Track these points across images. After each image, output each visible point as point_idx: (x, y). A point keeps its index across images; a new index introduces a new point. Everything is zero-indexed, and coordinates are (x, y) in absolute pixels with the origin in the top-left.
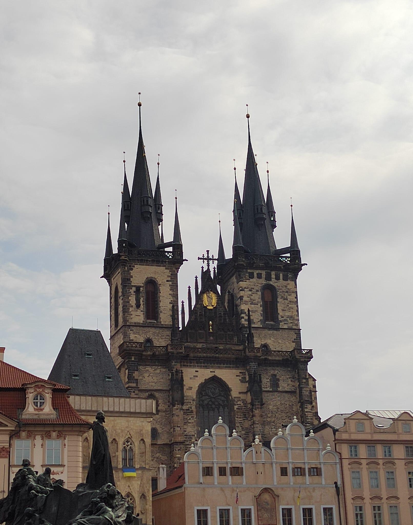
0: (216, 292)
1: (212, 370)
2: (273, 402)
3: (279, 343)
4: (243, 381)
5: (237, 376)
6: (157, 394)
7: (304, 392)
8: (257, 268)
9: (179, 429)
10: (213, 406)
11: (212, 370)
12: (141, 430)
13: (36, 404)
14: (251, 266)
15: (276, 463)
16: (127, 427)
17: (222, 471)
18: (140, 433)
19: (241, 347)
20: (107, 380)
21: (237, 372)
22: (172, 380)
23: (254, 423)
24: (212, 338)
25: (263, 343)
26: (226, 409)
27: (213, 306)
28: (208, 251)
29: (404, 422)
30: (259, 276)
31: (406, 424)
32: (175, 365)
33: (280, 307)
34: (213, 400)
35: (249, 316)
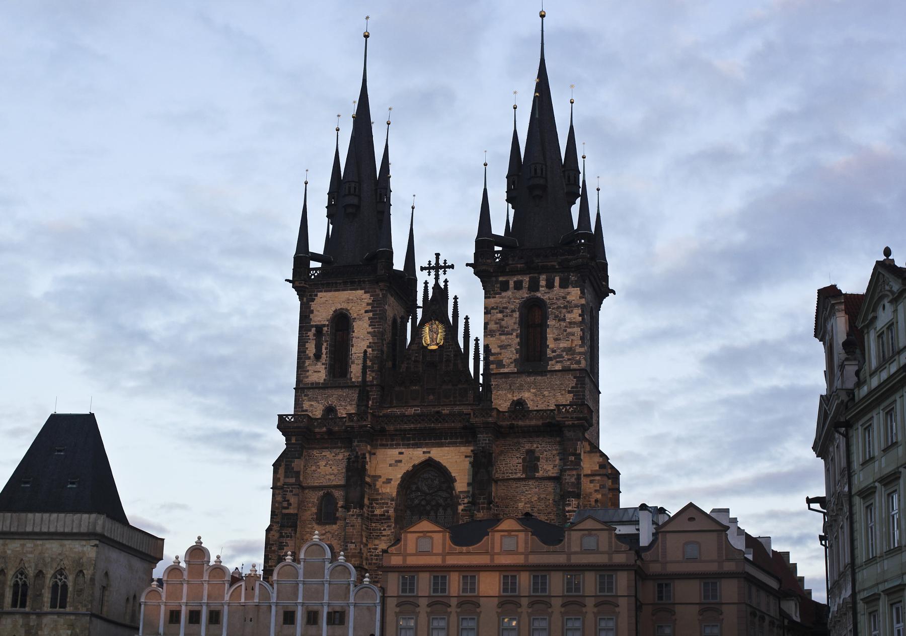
1: (425, 450)
3: (544, 396)
5: (466, 457)
6: (338, 494)
7: (568, 477)
8: (514, 272)
9: (353, 546)
10: (428, 508)
11: (425, 450)
12: (81, 558)
15: (277, 604)
16: (60, 554)
17: (194, 617)
20: (69, 486)
21: (467, 450)
24: (431, 397)
25: (515, 399)
26: (449, 511)
27: (437, 344)
28: (438, 255)
29: (506, 533)
30: (518, 286)
31: (510, 536)
32: (357, 446)
33: (550, 336)
34: (428, 498)
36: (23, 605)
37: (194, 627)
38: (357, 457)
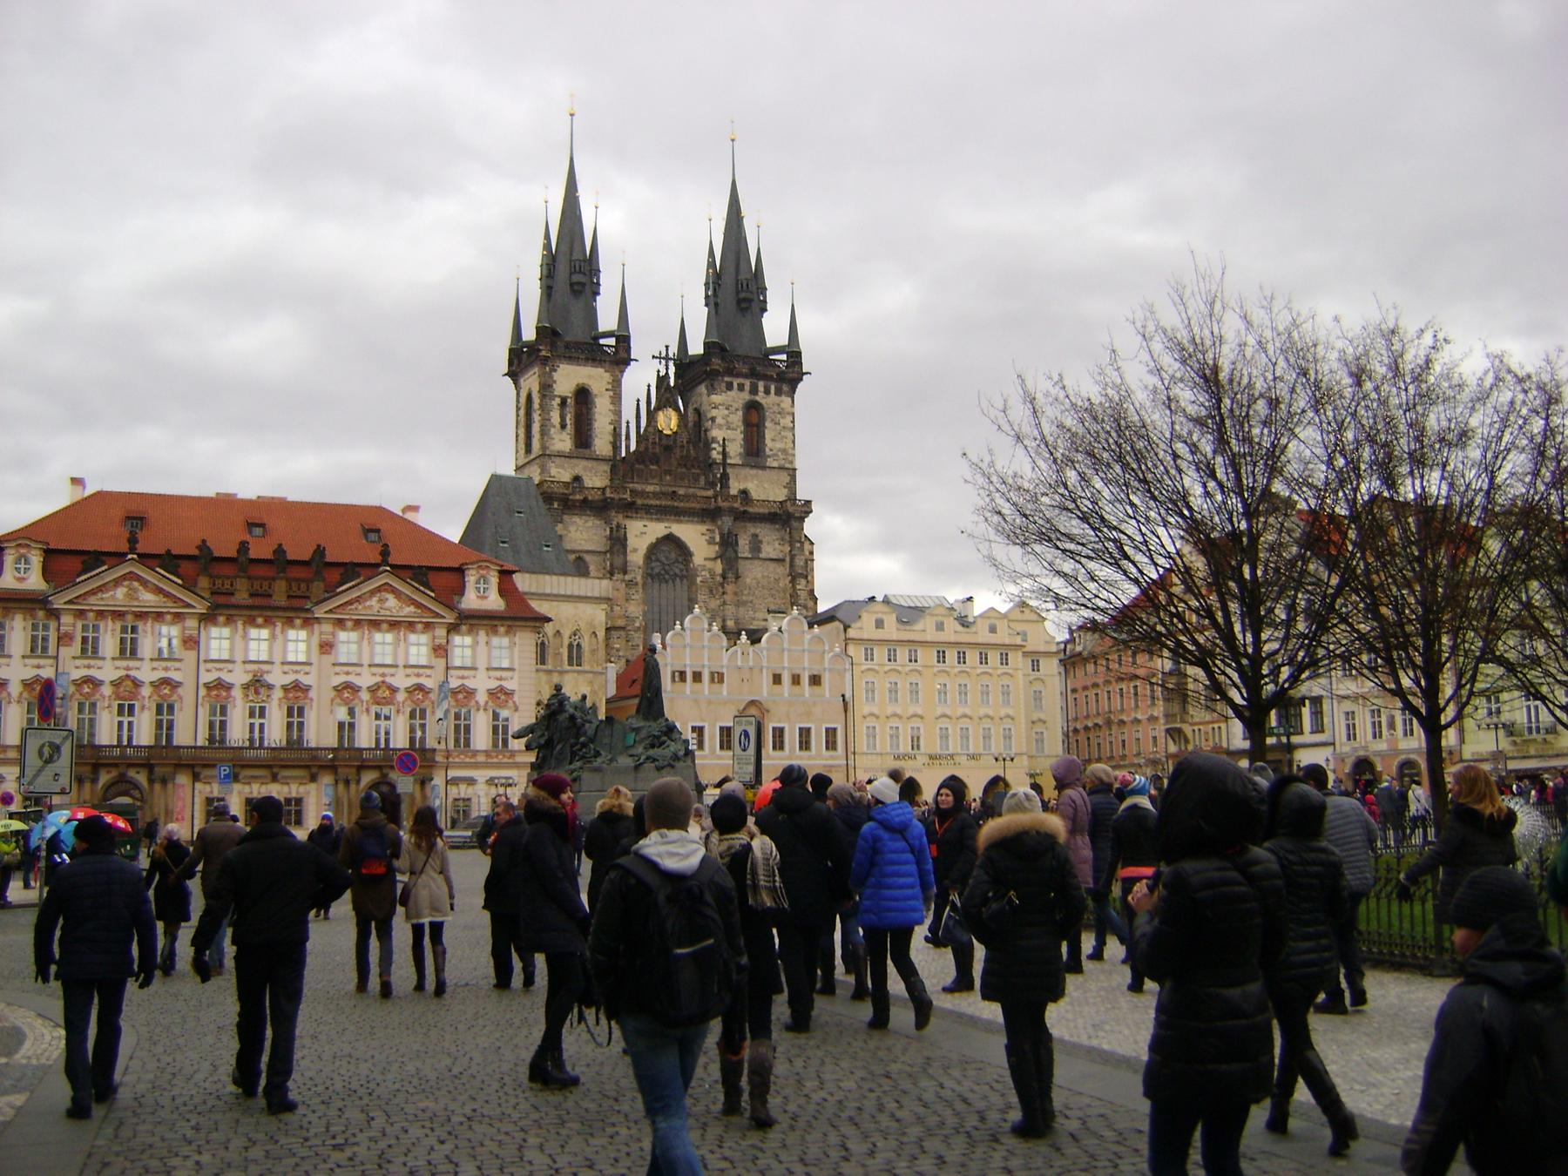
0: (677, 409)
2: (753, 573)
4: (711, 542)
6: (588, 558)
8: (738, 375)
13: (478, 589)
14: (731, 372)
17: (697, 677)
18: (591, 624)
19: (710, 493)
21: (703, 528)
22: (611, 538)
23: (724, 603)
30: (741, 388)
33: (768, 435)
35: (724, 446)
36: (543, 662)
37: (698, 685)
38: (618, 526)
